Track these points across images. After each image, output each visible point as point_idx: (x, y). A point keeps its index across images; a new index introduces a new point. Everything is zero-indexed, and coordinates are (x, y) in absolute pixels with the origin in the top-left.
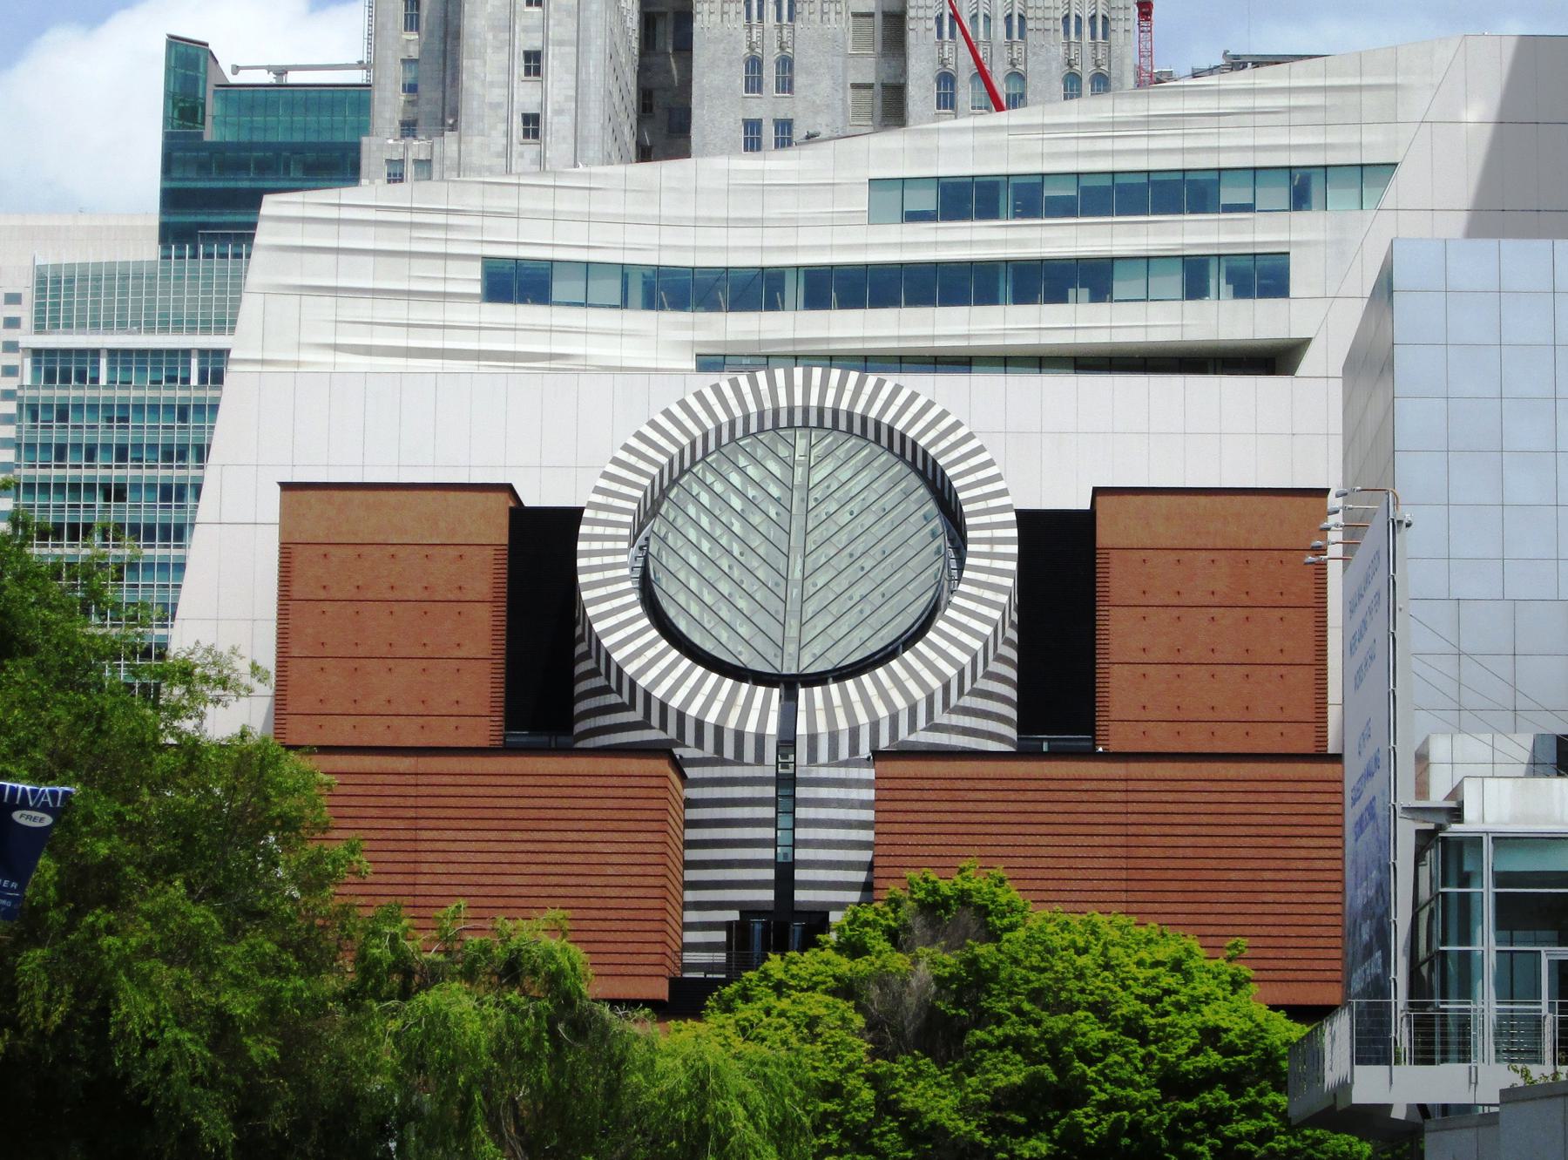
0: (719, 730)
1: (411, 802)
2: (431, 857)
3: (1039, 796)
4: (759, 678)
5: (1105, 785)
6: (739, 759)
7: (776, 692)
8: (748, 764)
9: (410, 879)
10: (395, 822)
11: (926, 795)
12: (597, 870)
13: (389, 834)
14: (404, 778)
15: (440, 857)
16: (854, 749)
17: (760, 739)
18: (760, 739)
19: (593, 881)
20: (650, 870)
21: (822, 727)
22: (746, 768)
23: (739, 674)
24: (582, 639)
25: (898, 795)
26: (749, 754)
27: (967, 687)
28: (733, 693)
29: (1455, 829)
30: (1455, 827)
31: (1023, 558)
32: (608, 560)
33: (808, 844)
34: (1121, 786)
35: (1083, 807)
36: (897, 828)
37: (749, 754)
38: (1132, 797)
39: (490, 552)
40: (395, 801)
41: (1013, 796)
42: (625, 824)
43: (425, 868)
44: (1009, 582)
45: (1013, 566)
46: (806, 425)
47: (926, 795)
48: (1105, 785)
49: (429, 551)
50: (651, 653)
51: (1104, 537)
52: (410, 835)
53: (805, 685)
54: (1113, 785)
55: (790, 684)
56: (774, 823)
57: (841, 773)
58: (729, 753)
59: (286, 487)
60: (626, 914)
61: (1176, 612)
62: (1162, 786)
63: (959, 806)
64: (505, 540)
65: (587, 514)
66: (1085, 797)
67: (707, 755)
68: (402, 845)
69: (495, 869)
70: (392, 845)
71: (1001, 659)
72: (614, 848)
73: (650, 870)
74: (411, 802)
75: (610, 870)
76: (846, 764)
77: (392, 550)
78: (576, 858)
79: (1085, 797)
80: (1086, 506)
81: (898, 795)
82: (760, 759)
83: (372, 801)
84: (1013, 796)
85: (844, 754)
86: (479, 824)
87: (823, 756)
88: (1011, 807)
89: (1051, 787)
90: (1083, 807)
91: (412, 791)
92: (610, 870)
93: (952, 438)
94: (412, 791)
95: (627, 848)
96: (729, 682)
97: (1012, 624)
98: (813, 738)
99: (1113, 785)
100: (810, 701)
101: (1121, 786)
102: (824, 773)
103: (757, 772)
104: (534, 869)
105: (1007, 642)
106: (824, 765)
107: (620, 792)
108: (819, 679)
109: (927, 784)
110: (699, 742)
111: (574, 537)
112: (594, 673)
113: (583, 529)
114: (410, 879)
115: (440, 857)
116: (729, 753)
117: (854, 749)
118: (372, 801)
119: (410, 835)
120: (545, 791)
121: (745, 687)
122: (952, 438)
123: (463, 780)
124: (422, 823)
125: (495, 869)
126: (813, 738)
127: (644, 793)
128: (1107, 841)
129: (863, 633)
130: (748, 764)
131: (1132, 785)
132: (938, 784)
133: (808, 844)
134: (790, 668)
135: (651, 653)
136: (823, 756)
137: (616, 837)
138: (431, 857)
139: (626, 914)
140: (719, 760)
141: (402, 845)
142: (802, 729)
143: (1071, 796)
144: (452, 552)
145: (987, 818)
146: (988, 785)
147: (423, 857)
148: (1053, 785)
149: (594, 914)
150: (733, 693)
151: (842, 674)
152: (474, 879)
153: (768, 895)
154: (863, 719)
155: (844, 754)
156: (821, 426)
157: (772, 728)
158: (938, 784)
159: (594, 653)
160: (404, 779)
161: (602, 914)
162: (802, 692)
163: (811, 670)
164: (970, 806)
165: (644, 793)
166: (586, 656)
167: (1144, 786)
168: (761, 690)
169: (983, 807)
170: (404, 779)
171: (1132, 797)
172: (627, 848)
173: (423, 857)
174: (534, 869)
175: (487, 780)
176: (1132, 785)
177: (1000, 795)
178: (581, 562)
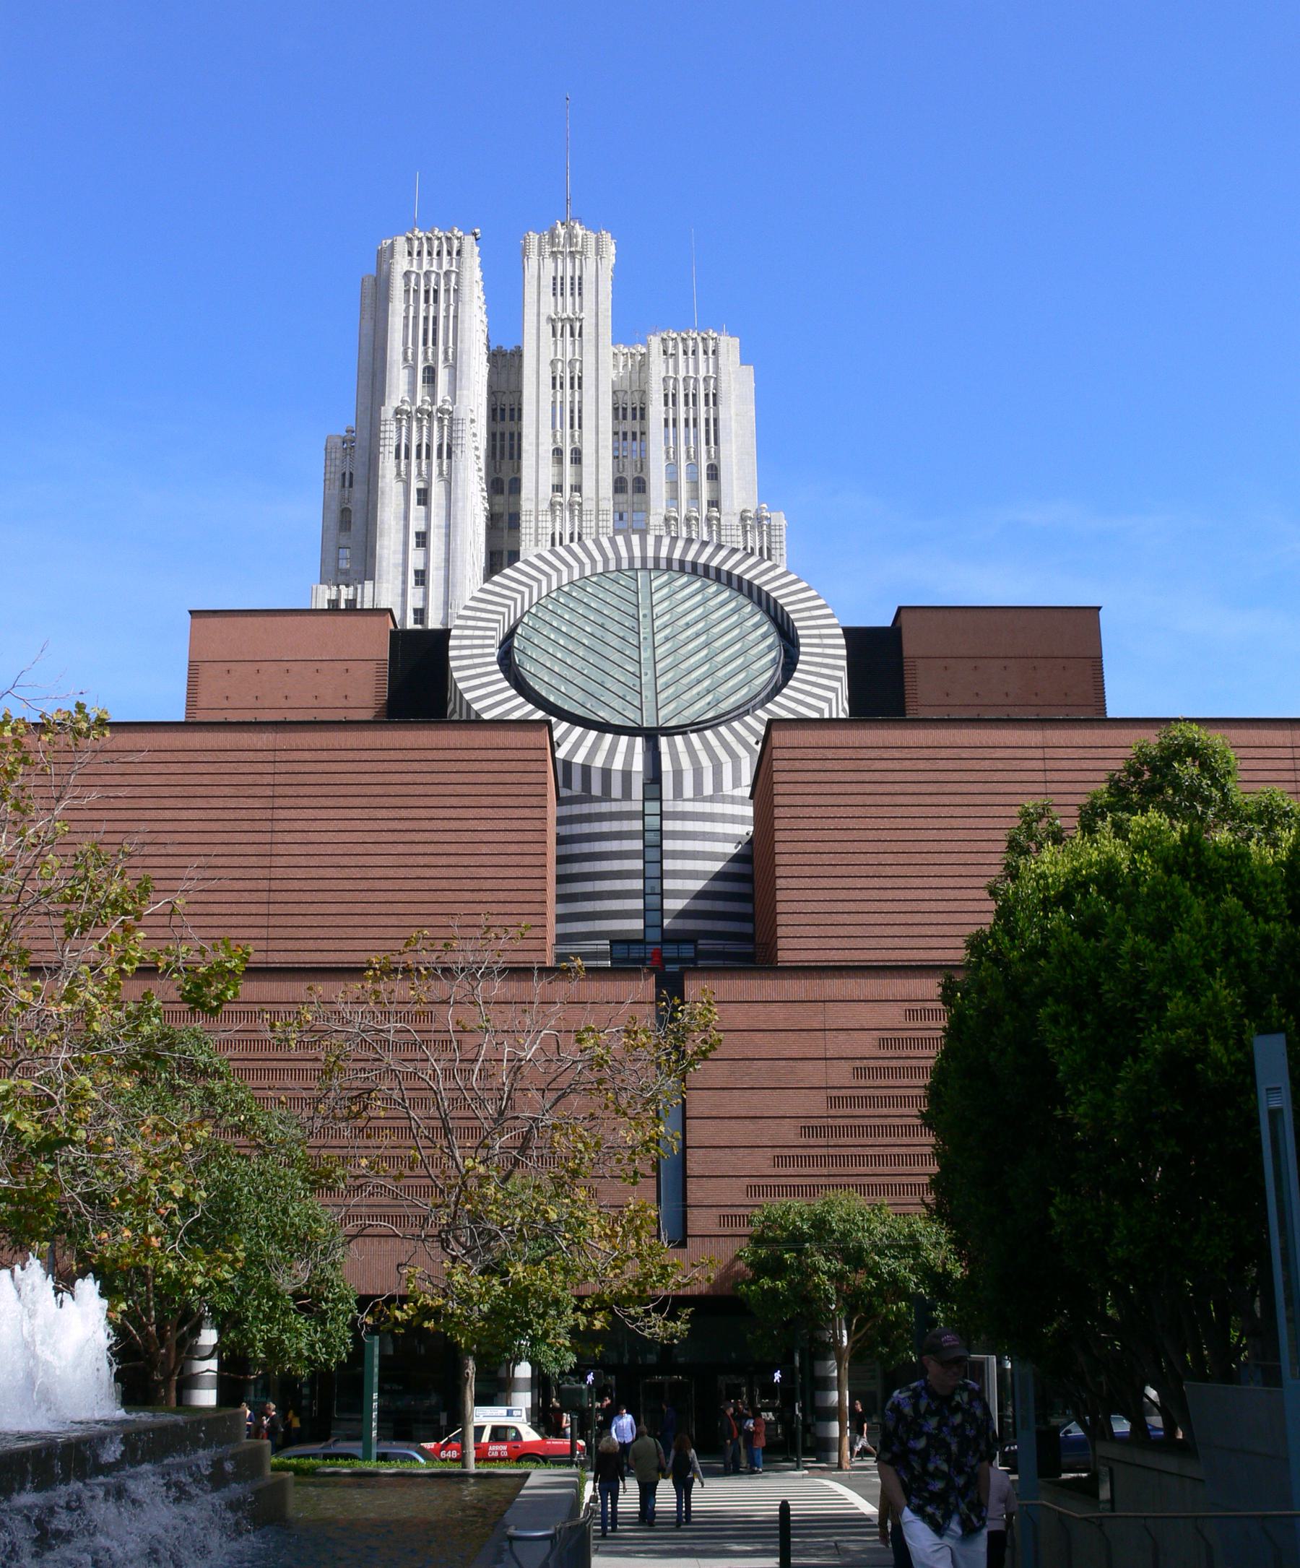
0: (586, 769)
1: (268, 779)
3: (951, 765)
4: (618, 730)
5: (1019, 753)
6: (606, 796)
7: (639, 741)
8: (616, 800)
9: (265, 861)
11: (829, 765)
14: (260, 754)
15: (298, 837)
16: (718, 784)
17: (627, 775)
22: (613, 803)
23: (604, 727)
24: (454, 711)
25: (798, 765)
26: (616, 791)
32: (476, 651)
34: (1039, 753)
38: (1050, 764)
39: (373, 665)
40: (250, 779)
41: (921, 765)
42: (501, 799)
44: (844, 663)
45: (844, 652)
46: (644, 568)
47: (829, 765)
48: (1019, 753)
49: (318, 665)
51: (909, 648)
52: (268, 814)
53: (663, 735)
54: (1029, 753)
55: (652, 736)
59: (191, 612)
60: (502, 896)
62: (1081, 753)
65: (453, 632)
66: (1000, 765)
67: (575, 793)
68: (257, 826)
74: (268, 779)
76: (711, 799)
79: (1000, 765)
80: (889, 624)
81: (798, 765)
82: (627, 795)
83: (226, 780)
85: (708, 789)
86: (342, 802)
88: (922, 777)
89: (964, 756)
93: (772, 574)
95: (503, 824)
96: (593, 734)
98: (678, 774)
99: (1029, 753)
100: (672, 747)
101: (1039, 753)
104: (401, 849)
107: (496, 766)
108: (681, 730)
109: (829, 754)
110: (568, 784)
113: (452, 643)
114: (265, 861)
115: (298, 837)
116: (596, 790)
117: (718, 784)
118: (226, 780)
119: (268, 814)
121: (609, 737)
122: (772, 574)
124: (279, 802)
127: (520, 766)
130: (616, 800)
133: (676, 874)
136: (688, 791)
139: (502, 896)
140: (587, 797)
141: (257, 826)
142: (666, 765)
144: (341, 666)
145: (897, 788)
146: (896, 754)
147: (279, 837)
149: (467, 896)
152: (336, 860)
153: (638, 924)
155: (708, 789)
156: (657, 567)
157: (638, 765)
160: (260, 757)
162: (663, 741)
164: (877, 777)
168: (624, 740)
170: (260, 757)
171: (1050, 764)
172: (503, 824)
173: (279, 837)
174: (401, 849)
175: (351, 755)
176: (1049, 753)
177: (907, 764)
178: (452, 653)
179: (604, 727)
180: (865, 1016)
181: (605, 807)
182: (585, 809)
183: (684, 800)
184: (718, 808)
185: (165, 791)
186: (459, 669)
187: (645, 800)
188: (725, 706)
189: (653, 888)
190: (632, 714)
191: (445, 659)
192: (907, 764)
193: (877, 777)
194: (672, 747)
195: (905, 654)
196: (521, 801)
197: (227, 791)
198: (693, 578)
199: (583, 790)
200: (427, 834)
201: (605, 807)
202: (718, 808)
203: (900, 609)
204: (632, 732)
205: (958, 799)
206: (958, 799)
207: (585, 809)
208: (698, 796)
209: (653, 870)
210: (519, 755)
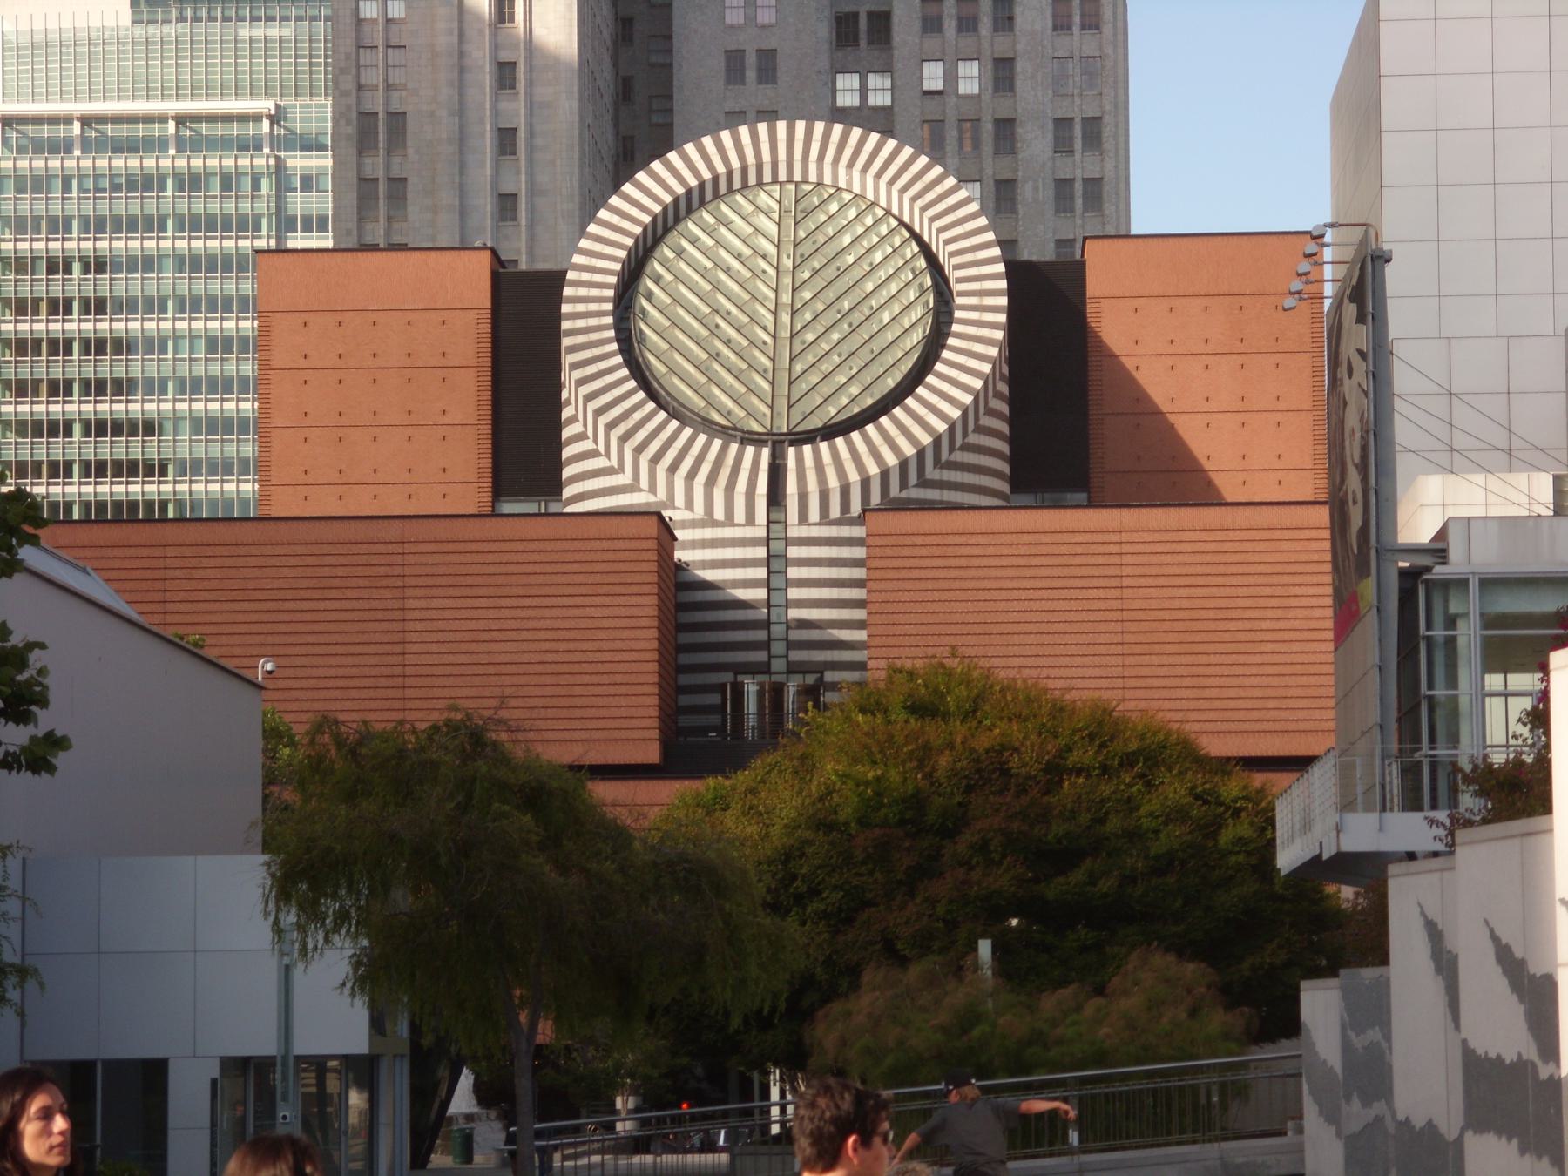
1: (397, 571)
2: (419, 626)
4: (748, 438)
6: (729, 521)
7: (766, 452)
9: (398, 649)
10: (382, 591)
12: (589, 634)
13: (374, 604)
19: (586, 646)
20: (639, 633)
24: (568, 402)
25: (889, 552)
26: (740, 515)
27: (959, 443)
28: (724, 450)
29: (1439, 571)
30: (1438, 569)
31: (1014, 311)
32: (593, 322)
34: (1115, 537)
35: (1077, 560)
36: (889, 585)
37: (740, 515)
38: (1126, 548)
39: (472, 315)
40: (382, 571)
43: (413, 637)
44: (999, 335)
50: (638, 416)
53: (791, 445)
55: (778, 442)
57: (833, 531)
58: (719, 514)
61: (1170, 361)
62: (1157, 537)
63: (952, 562)
64: (489, 305)
65: (571, 275)
66: (1079, 549)
67: (697, 517)
69: (486, 636)
70: (380, 615)
71: (991, 412)
72: (606, 612)
73: (639, 633)
75: (601, 635)
77: (373, 317)
78: (567, 624)
79: (1079, 549)
82: (750, 520)
84: (1005, 550)
87: (814, 515)
90: (1077, 560)
91: (399, 560)
92: (601, 635)
94: (399, 560)
97: (1002, 377)
98: (803, 497)
101: (1115, 537)
102: (816, 532)
103: (749, 532)
105: (998, 395)
106: (815, 524)
107: (610, 556)
108: (810, 437)
110: (689, 505)
111: (558, 299)
112: (582, 437)
116: (719, 514)
118: (359, 571)
120: (536, 557)
123: (451, 547)
125: (486, 636)
126: (803, 497)
127: (632, 556)
128: (1102, 593)
131: (1125, 537)
132: (929, 540)
135: (638, 416)
136: (814, 515)
137: (607, 600)
138: (419, 626)
143: (1064, 549)
145: (980, 573)
148: (1045, 539)
149: (586, 679)
150: (724, 450)
151: (830, 432)
152: (464, 647)
154: (854, 476)
155: (835, 512)
158: (929, 540)
159: (581, 417)
160: (391, 548)
161: (595, 679)
162: (791, 451)
163: (800, 428)
164: (963, 562)
165: (632, 556)
166: (573, 419)
167: (1135, 537)
169: (976, 562)
170: (391, 548)
176: (1125, 537)
177: (991, 550)
181: (728, 533)
182: (708, 533)
183: (809, 525)
185: (305, 583)
186: (573, 349)
187: (769, 522)
189: (779, 616)
191: (555, 335)
192: (991, 550)
193: (963, 562)
195: (1090, 292)
196: (635, 589)
197: (361, 582)
199: (706, 514)
200: (548, 621)
201: (728, 533)
205: (1038, 584)
206: (1038, 584)
207: (708, 533)
208: (825, 519)
209: (777, 599)
210: (633, 545)
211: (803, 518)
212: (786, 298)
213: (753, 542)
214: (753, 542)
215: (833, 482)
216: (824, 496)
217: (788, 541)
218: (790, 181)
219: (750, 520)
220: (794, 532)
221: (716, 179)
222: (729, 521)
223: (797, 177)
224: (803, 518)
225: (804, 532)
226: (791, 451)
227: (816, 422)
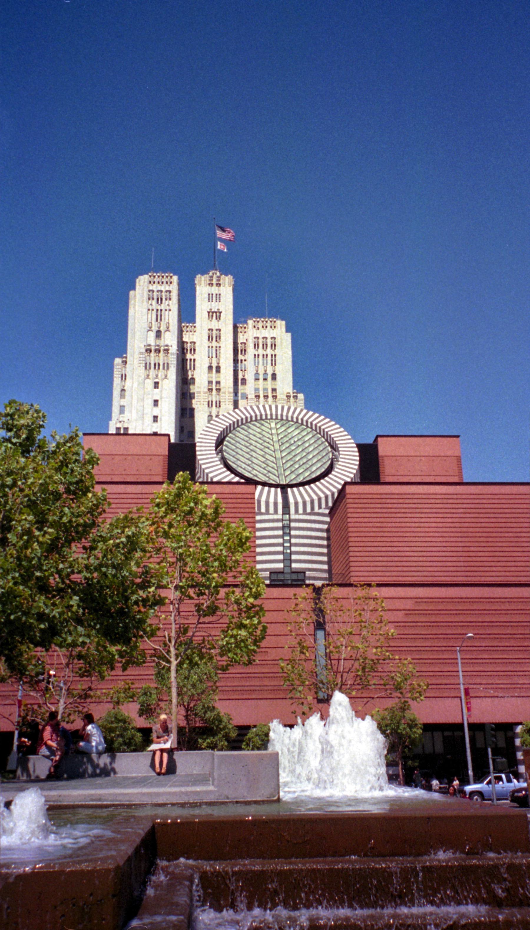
4: (270, 486)
6: (267, 512)
7: (279, 490)
16: (312, 508)
17: (276, 504)
18: (276, 504)
21: (300, 500)
26: (271, 510)
33: (296, 545)
37: (271, 510)
39: (161, 457)
55: (284, 488)
56: (282, 537)
64: (167, 453)
76: (309, 514)
82: (276, 512)
85: (309, 510)
87: (301, 510)
98: (296, 503)
100: (293, 492)
103: (275, 517)
117: (312, 508)
126: (296, 503)
129: (307, 474)
133: (296, 545)
134: (283, 482)
136: (301, 510)
142: (291, 500)
144: (149, 458)
151: (302, 484)
153: (281, 565)
155: (309, 510)
156: (277, 418)
162: (289, 490)
168: (273, 489)
178: (198, 453)
179: (264, 484)
180: (398, 604)
184: (313, 518)
188: (314, 476)
190: (277, 479)
194: (293, 492)
198: (292, 423)
202: (313, 518)
203: (377, 437)
204: (276, 486)
208: (305, 512)
211: (297, 511)
212: (277, 446)
213: (277, 521)
214: (277, 521)
215: (307, 499)
216: (304, 503)
217: (290, 520)
218: (272, 418)
219: (276, 512)
220: (293, 517)
221: (247, 418)
222: (267, 512)
223: (274, 417)
224: (297, 511)
225: (297, 517)
226: (289, 490)
227: (294, 482)
